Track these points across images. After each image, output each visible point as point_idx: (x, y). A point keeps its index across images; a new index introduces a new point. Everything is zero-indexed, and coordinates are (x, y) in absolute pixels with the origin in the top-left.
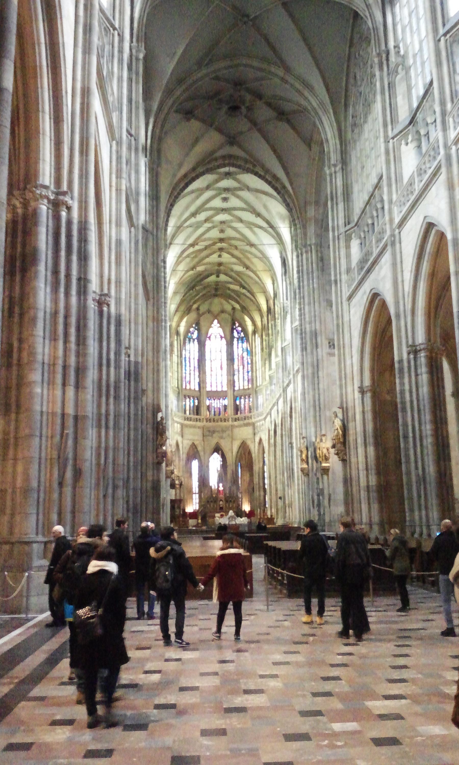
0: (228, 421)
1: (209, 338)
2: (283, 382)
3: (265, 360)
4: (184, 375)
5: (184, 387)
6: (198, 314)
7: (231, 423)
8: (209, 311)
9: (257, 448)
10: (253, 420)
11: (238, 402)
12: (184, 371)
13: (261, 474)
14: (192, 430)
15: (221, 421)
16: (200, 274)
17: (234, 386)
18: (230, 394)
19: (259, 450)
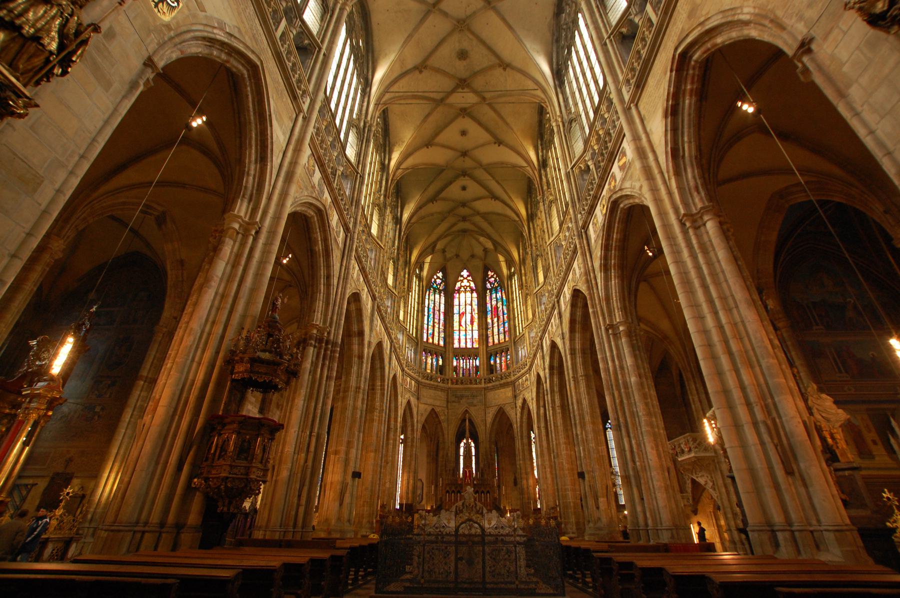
0: (480, 383)
1: (459, 291)
2: (576, 222)
3: (526, 297)
4: (425, 326)
5: (425, 340)
6: (445, 259)
7: (483, 385)
8: (457, 256)
9: (519, 415)
10: (513, 378)
11: (492, 362)
12: (426, 322)
13: (526, 453)
14: (432, 392)
15: (471, 383)
16: (439, 170)
17: (487, 342)
18: (483, 353)
19: (521, 418)
